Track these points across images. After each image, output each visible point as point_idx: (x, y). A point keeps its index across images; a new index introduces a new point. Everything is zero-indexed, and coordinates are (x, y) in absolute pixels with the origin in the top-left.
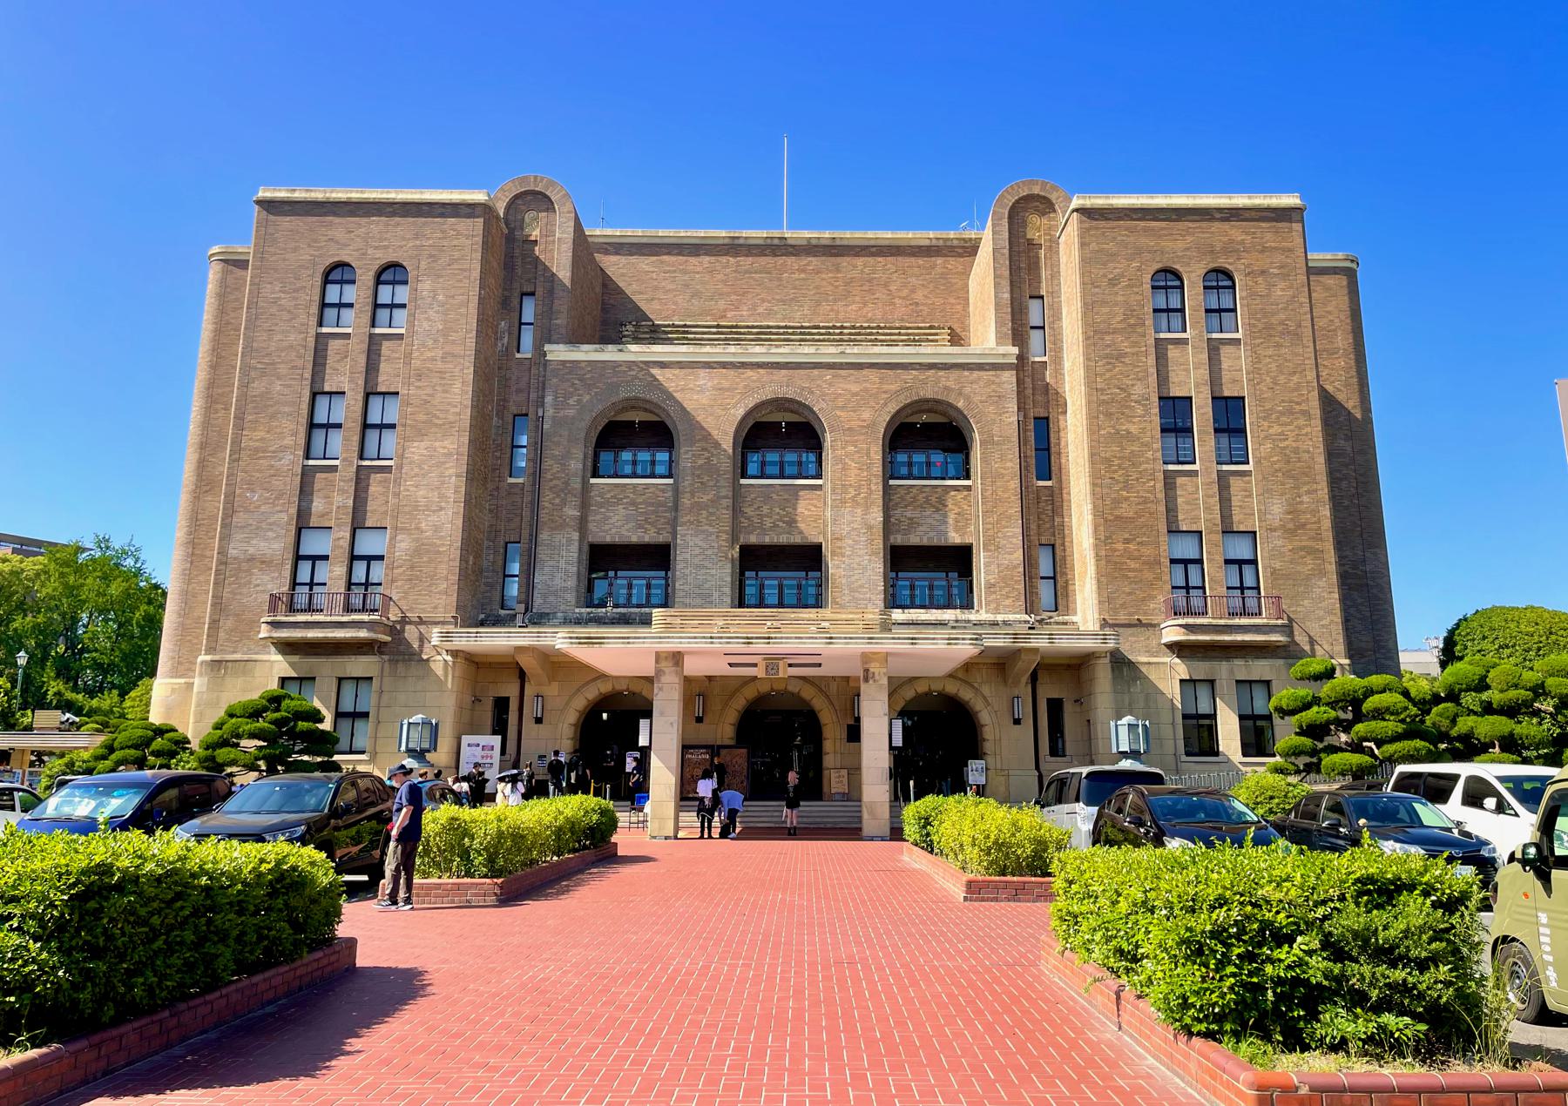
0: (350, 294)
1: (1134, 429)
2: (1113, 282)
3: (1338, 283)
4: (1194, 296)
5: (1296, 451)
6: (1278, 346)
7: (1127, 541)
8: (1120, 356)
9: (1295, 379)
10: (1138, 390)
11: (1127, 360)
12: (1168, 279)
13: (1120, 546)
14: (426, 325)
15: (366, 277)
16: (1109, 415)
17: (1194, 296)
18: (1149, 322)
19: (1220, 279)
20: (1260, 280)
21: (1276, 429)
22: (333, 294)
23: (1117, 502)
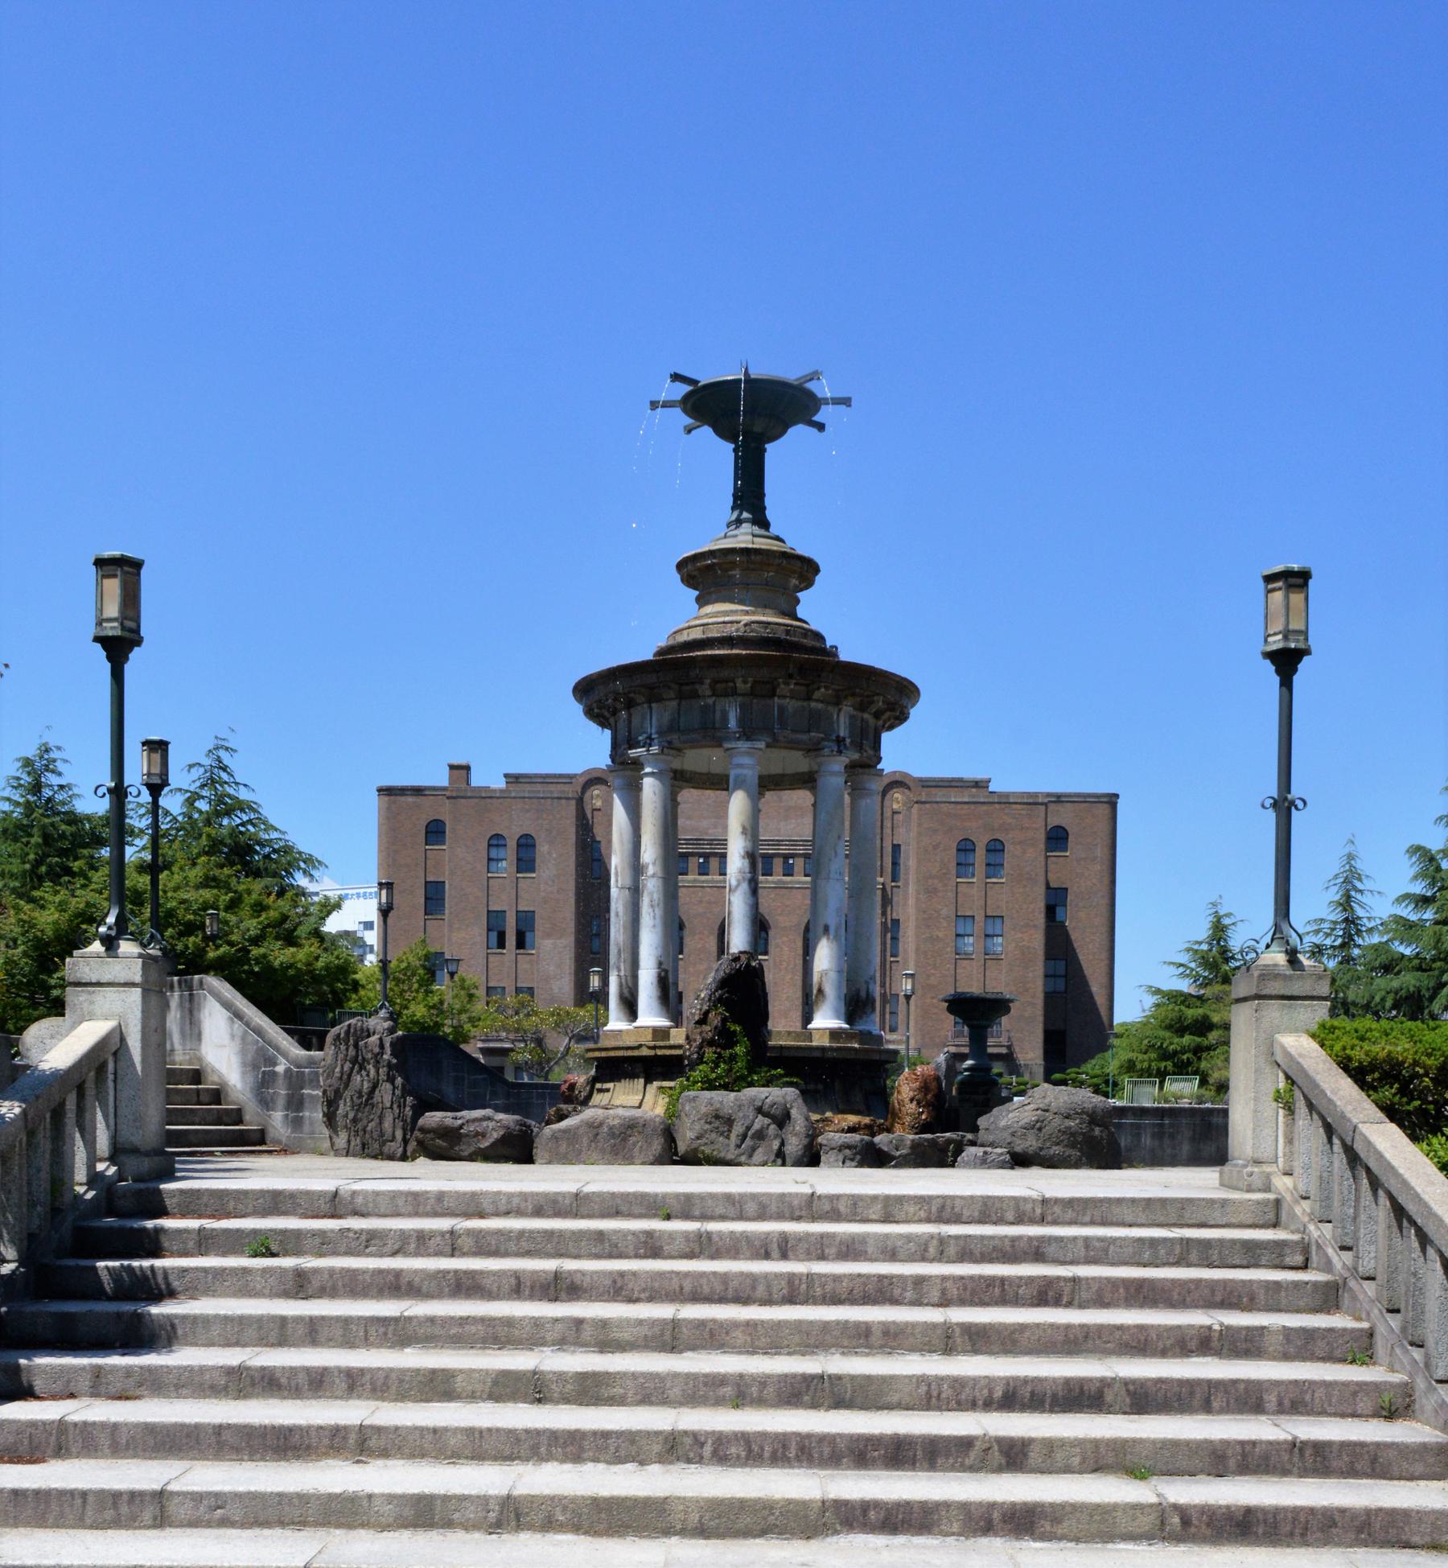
0: (502, 853)
1: (941, 935)
2: (936, 847)
3: (1104, 810)
4: (980, 856)
5: (1028, 948)
6: (1025, 886)
7: (933, 998)
8: (935, 891)
9: (1032, 906)
10: (944, 912)
11: (940, 894)
12: (966, 848)
13: (928, 1001)
14: (547, 872)
15: (512, 844)
16: (928, 927)
17: (980, 856)
18: (954, 872)
19: (996, 848)
20: (1018, 847)
21: (1020, 935)
22: (494, 853)
23: (929, 976)
